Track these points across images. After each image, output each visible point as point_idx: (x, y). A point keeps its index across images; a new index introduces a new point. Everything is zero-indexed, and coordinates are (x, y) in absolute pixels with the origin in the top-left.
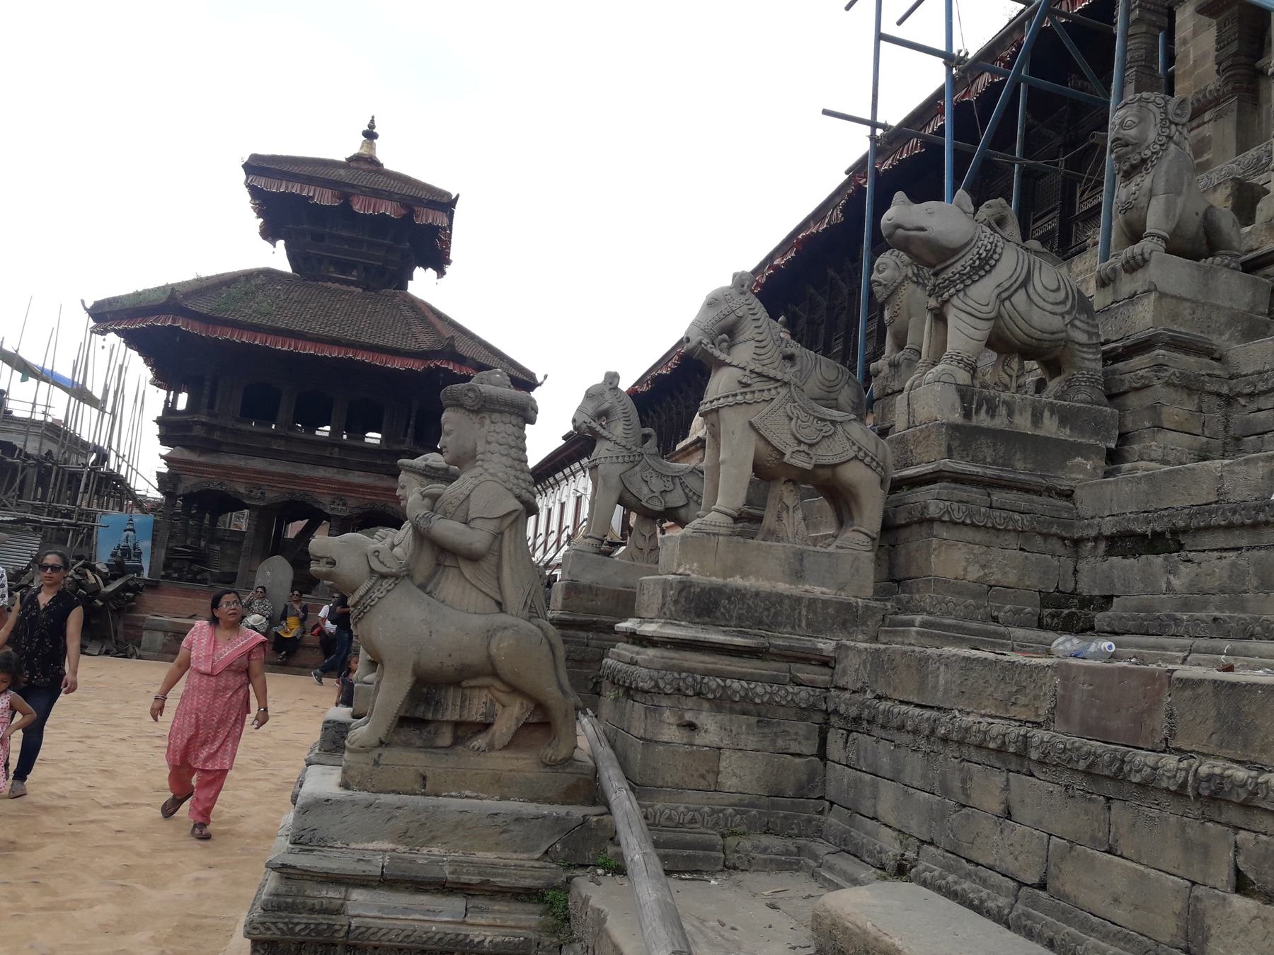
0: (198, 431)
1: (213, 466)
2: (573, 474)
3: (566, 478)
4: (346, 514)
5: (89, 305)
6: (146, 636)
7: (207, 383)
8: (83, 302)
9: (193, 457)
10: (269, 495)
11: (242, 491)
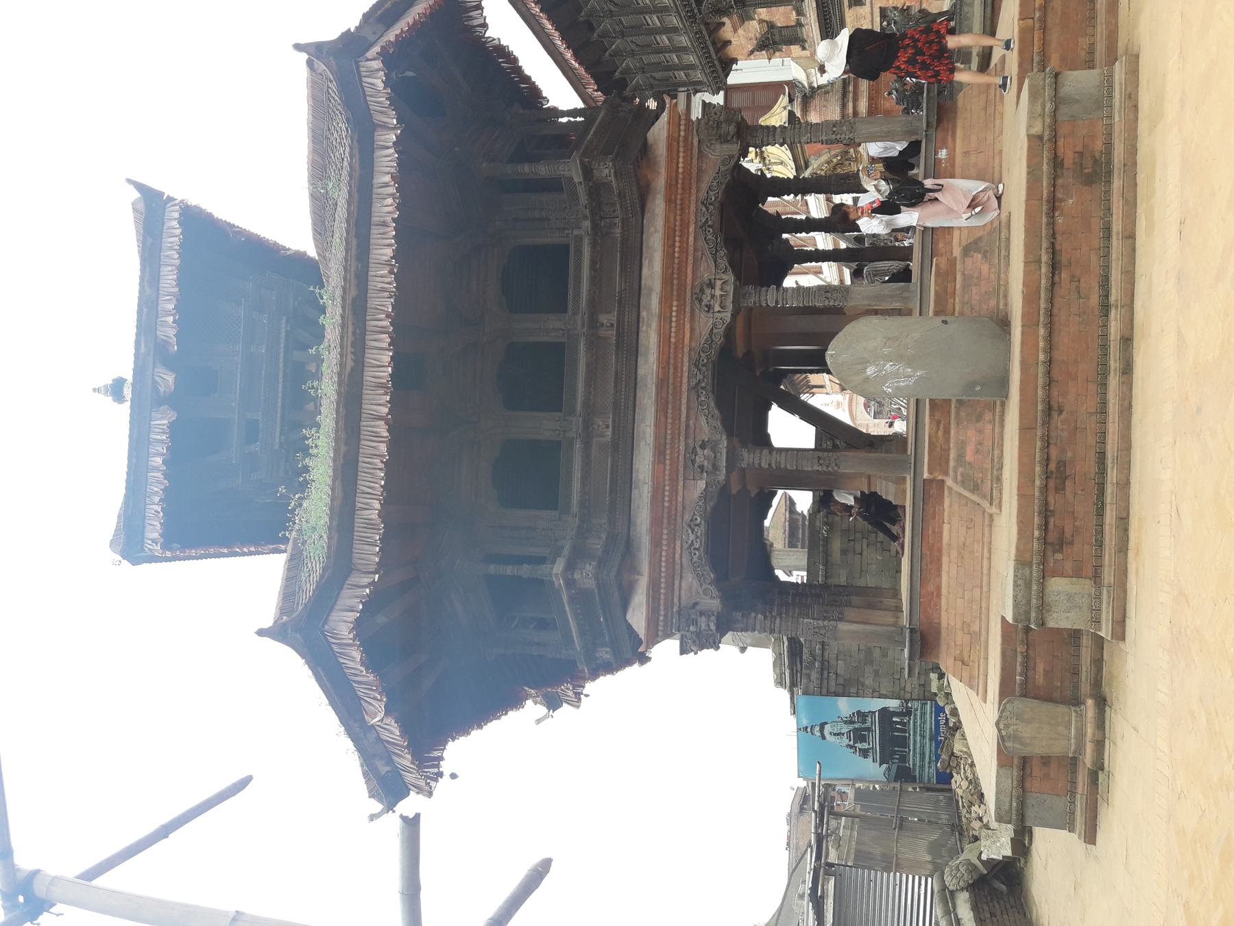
0: (586, 575)
1: (656, 543)
4: (730, 277)
5: (377, 807)
6: (1060, 620)
8: (372, 817)
9: (643, 583)
11: (702, 485)
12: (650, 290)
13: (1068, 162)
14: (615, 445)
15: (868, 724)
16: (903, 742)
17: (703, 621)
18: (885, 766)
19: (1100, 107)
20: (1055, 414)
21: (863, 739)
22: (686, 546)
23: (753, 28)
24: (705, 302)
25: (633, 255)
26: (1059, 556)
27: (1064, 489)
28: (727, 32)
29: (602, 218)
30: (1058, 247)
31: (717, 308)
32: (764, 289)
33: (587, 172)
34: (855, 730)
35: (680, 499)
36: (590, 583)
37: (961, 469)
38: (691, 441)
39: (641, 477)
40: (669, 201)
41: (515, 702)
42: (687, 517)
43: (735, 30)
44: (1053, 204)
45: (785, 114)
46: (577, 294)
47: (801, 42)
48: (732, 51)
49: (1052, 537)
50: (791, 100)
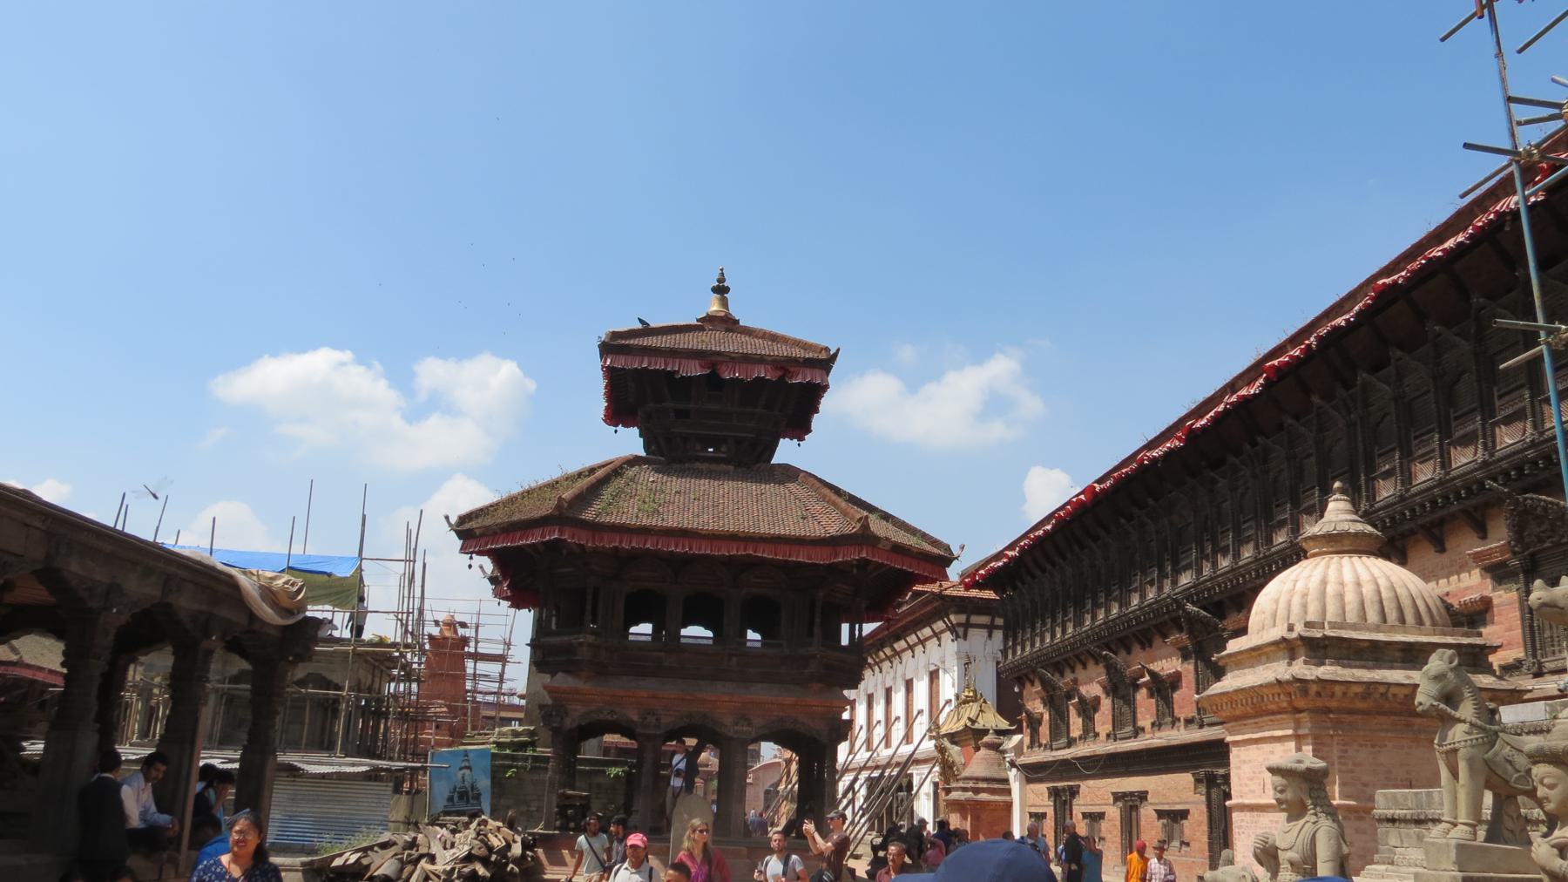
2: (922, 642)
3: (911, 647)
5: (453, 520)
8: (447, 518)
10: (665, 720)
11: (635, 718)
34: (466, 793)
47: (1031, 746)
50: (999, 733)
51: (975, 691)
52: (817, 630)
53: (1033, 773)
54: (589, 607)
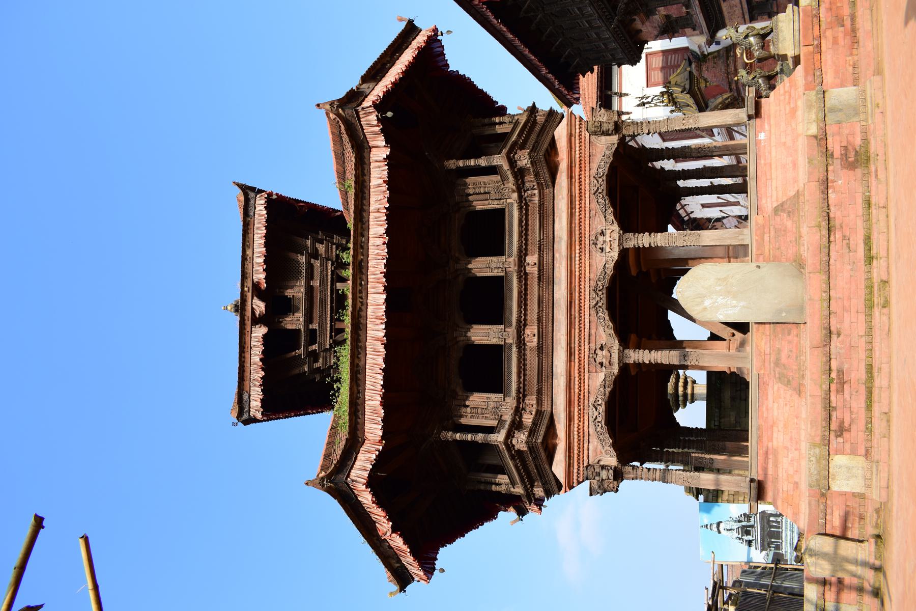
1: (570, 419)
4: (616, 227)
5: (395, 587)
7: (458, 436)
11: (601, 376)
12: (561, 238)
13: (837, 154)
14: (540, 348)
15: (752, 523)
16: (778, 535)
17: (604, 474)
18: (764, 552)
19: (857, 114)
20: (834, 337)
21: (748, 533)
22: (591, 420)
23: (658, 18)
24: (599, 246)
25: (546, 215)
26: (840, 440)
27: (843, 391)
28: (638, 24)
29: (525, 191)
30: (832, 215)
31: (608, 250)
32: (641, 235)
33: (512, 163)
34: (743, 527)
35: (586, 387)
36: (523, 447)
37: (778, 369)
38: (593, 345)
39: (559, 371)
40: (571, 177)
41: (491, 515)
42: (592, 400)
43: (643, 23)
44: (826, 185)
45: (687, 74)
46: (511, 242)
48: (644, 36)
49: (833, 427)
51: (662, 94)
52: (483, 162)
53: (715, 23)
54: (469, 437)
